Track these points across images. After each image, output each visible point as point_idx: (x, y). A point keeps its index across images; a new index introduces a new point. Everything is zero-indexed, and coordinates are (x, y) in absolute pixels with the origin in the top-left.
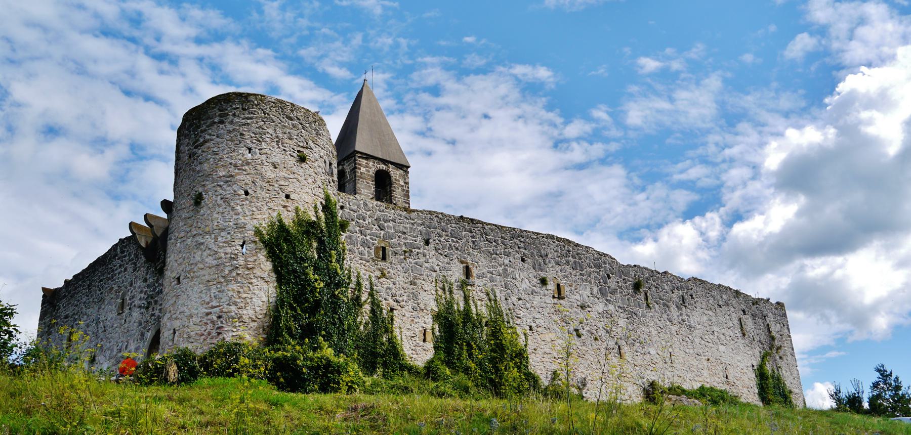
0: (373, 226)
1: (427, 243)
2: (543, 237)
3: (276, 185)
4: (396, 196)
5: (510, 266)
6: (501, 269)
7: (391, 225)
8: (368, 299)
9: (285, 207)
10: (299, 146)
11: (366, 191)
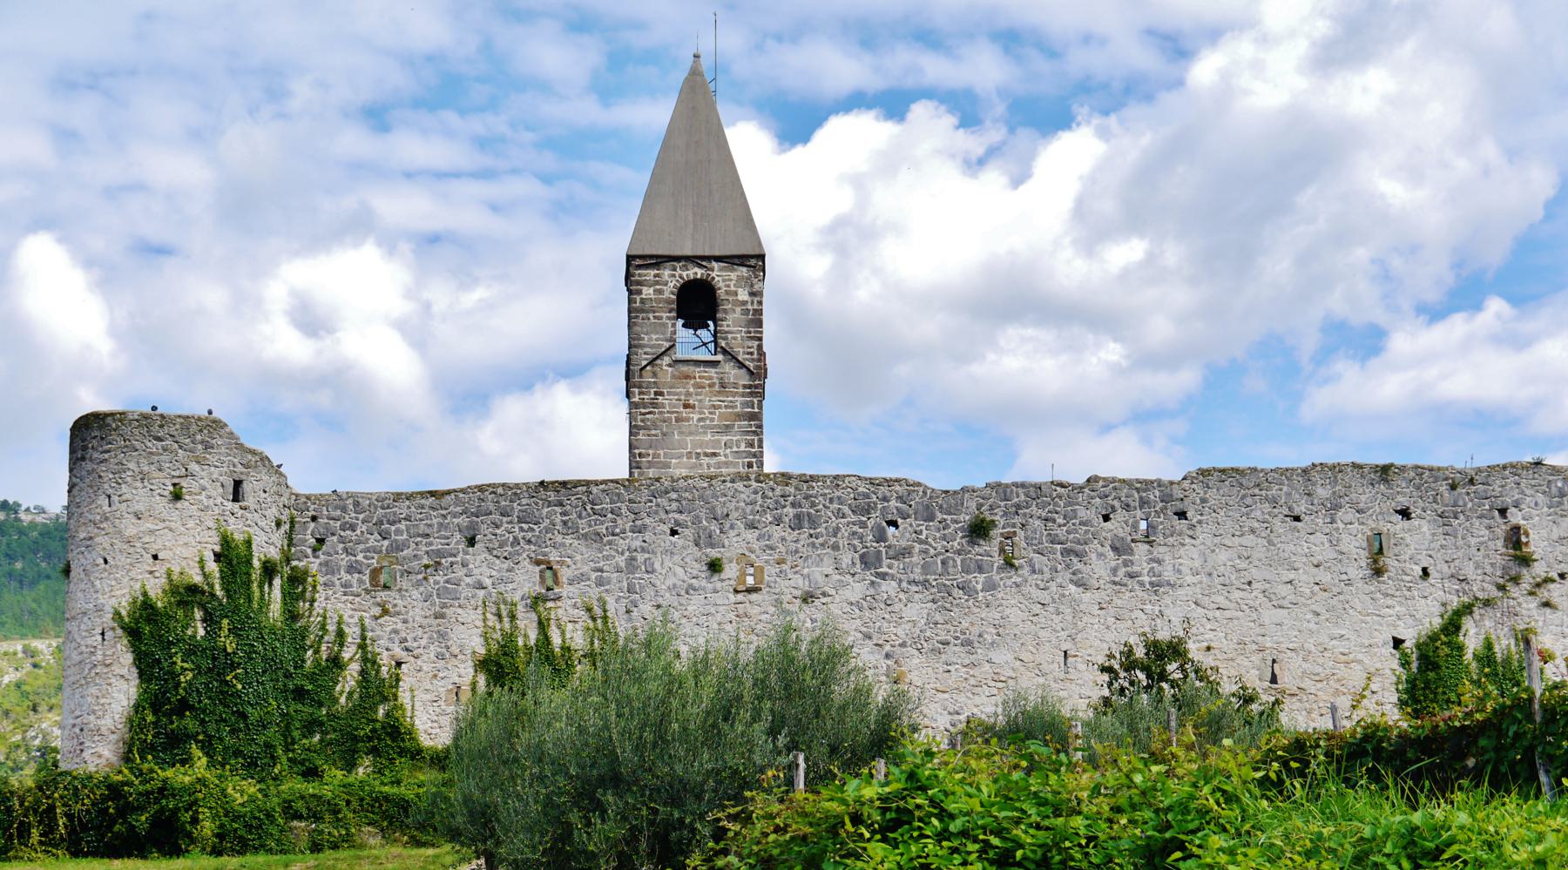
0: (369, 536)
1: (471, 542)
2: (724, 481)
3: (138, 545)
4: (726, 329)
5: (643, 550)
6: (621, 561)
7: (403, 527)
8: (357, 653)
9: (151, 572)
10: (174, 477)
11: (654, 337)
